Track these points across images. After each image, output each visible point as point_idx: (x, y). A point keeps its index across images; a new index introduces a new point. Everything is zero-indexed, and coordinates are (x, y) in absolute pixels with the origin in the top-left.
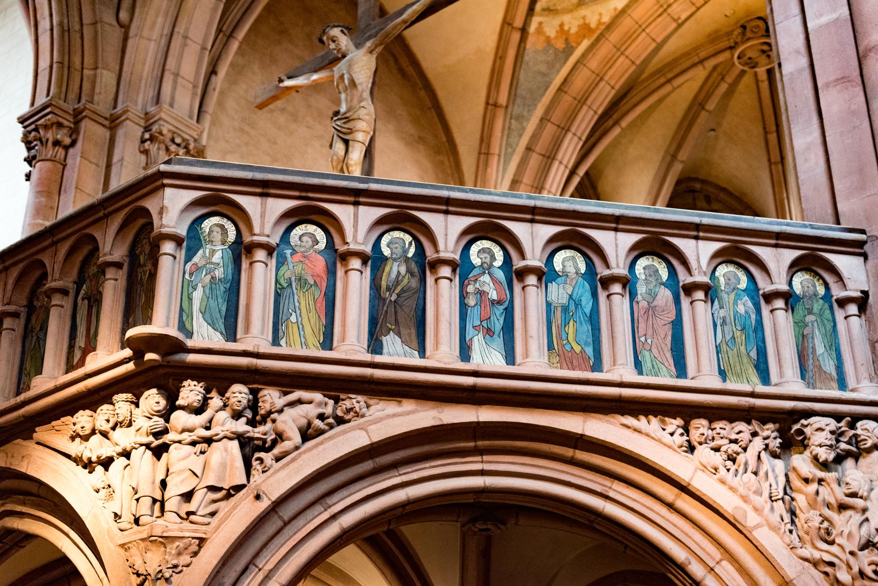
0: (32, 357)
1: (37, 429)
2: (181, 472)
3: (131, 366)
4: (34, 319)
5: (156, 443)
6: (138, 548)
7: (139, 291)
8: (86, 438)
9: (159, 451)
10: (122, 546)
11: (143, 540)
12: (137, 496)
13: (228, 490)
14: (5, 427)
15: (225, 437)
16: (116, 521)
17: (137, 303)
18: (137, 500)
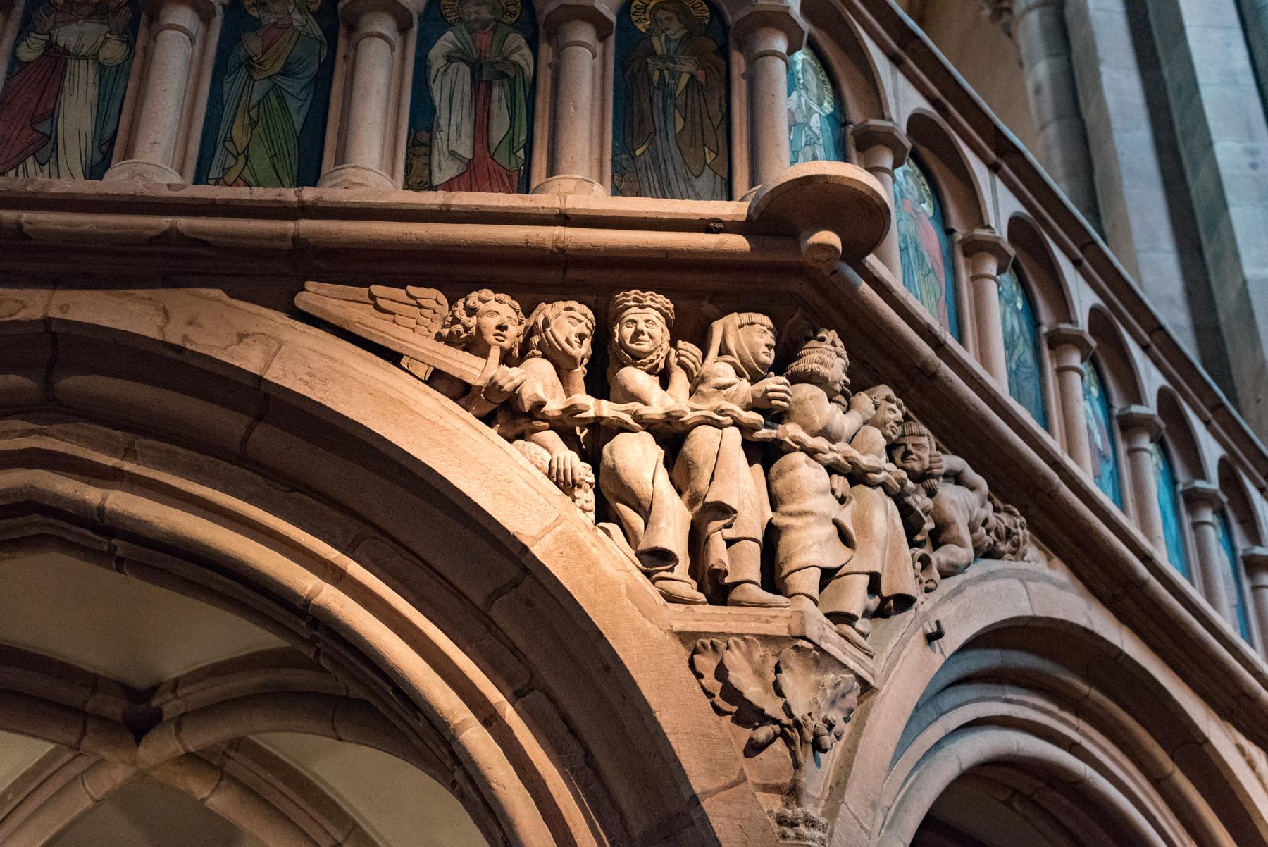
0: (253, 124)
1: (310, 285)
2: (822, 517)
4: (253, 44)
5: (764, 433)
6: (748, 656)
7: (658, 102)
10: (685, 637)
11: (766, 639)
12: (729, 533)
13: (884, 600)
14: (205, 244)
15: (884, 485)
16: (648, 575)
17: (659, 124)
18: (730, 542)
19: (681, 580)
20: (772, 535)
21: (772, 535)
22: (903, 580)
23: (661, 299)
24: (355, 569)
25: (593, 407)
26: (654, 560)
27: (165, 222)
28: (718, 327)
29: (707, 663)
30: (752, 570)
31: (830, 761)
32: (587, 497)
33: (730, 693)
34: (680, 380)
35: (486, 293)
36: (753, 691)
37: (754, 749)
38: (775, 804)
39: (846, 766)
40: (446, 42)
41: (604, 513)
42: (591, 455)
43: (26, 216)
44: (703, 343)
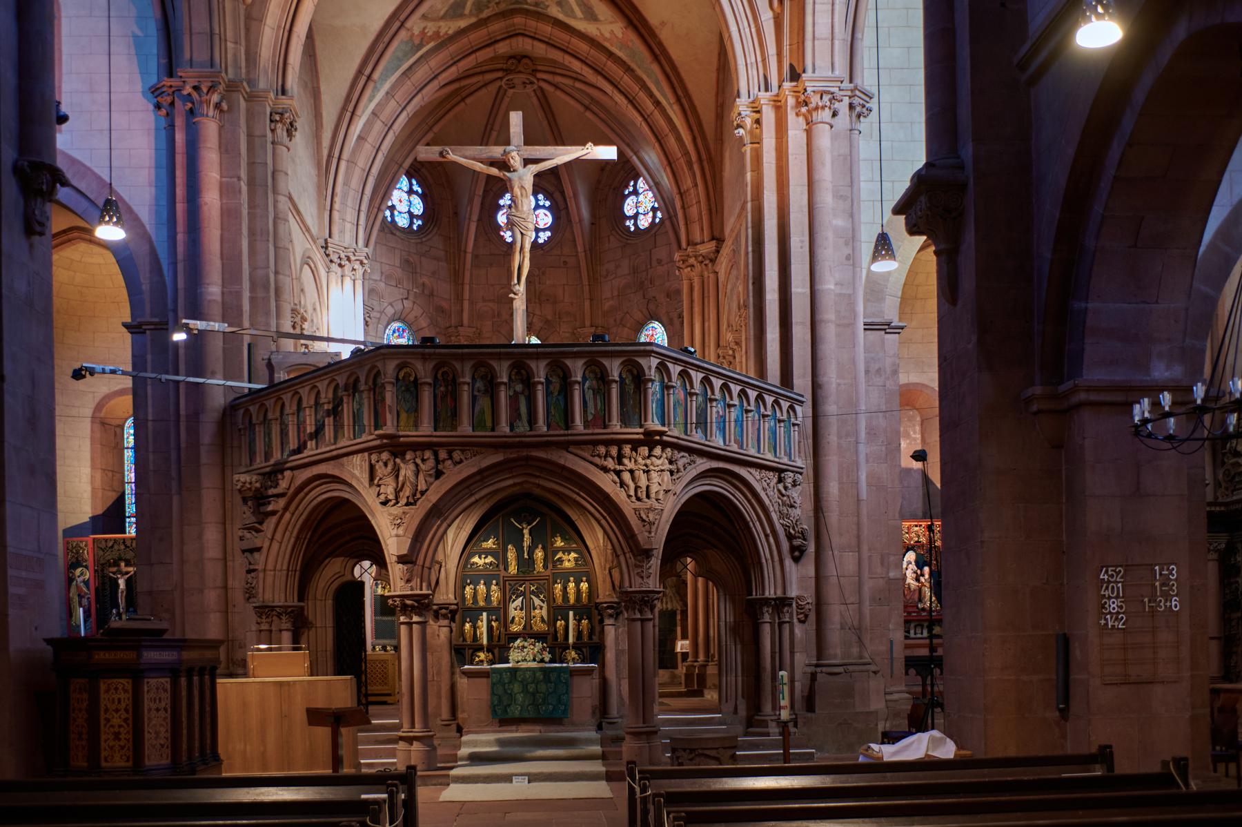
3: (642, 437)
4: (551, 387)
8: (606, 457)
9: (647, 472)
10: (634, 509)
19: (634, 499)
20: (648, 487)
21: (648, 487)
22: (671, 487)
23: (630, 446)
24: (581, 493)
25: (619, 468)
26: (629, 496)
27: (546, 439)
28: (639, 449)
29: (637, 513)
30: (644, 496)
31: (656, 525)
32: (618, 485)
33: (641, 518)
34: (633, 460)
35: (600, 446)
36: (644, 517)
37: (644, 526)
38: (647, 534)
39: (658, 525)
40: (587, 384)
41: (621, 487)
42: (619, 477)
43: (523, 439)
44: (637, 453)
